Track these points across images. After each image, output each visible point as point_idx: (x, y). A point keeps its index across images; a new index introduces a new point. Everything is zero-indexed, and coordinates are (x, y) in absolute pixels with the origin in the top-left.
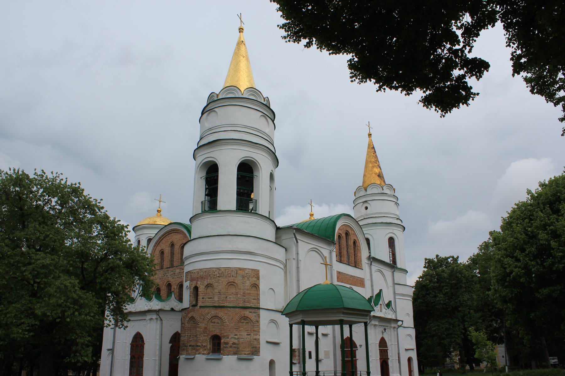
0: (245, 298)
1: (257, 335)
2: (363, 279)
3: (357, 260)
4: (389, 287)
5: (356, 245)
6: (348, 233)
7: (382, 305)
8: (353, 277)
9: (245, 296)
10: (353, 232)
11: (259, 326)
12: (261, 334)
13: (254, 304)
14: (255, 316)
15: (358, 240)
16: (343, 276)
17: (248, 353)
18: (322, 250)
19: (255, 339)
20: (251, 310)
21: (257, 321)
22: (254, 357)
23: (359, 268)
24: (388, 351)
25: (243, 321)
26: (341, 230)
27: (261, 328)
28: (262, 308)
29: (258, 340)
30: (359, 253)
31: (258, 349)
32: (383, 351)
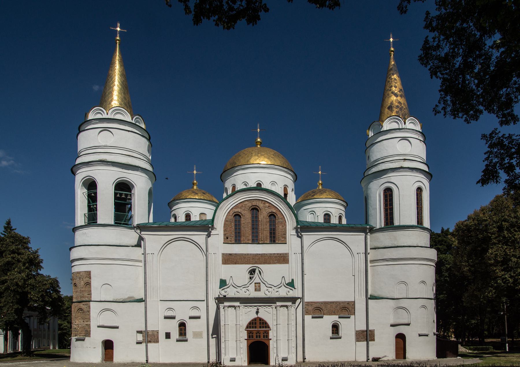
0: (81, 294)
1: (88, 322)
2: (286, 254)
3: (277, 234)
4: (355, 254)
5: (277, 217)
6: (257, 207)
7: (261, 283)
8: (260, 256)
9: (81, 293)
10: (267, 205)
11: (89, 315)
12: (91, 320)
13: (88, 298)
14: (86, 307)
15: (280, 211)
16: (238, 257)
17: (83, 335)
18: (194, 238)
19: (86, 325)
20: (83, 303)
21: (88, 311)
22: (87, 338)
23: (279, 242)
24: (270, 331)
25: (80, 311)
26: (241, 208)
27: (91, 316)
28: (94, 300)
29: (89, 326)
30: (281, 227)
31: (89, 332)
32: (255, 332)
